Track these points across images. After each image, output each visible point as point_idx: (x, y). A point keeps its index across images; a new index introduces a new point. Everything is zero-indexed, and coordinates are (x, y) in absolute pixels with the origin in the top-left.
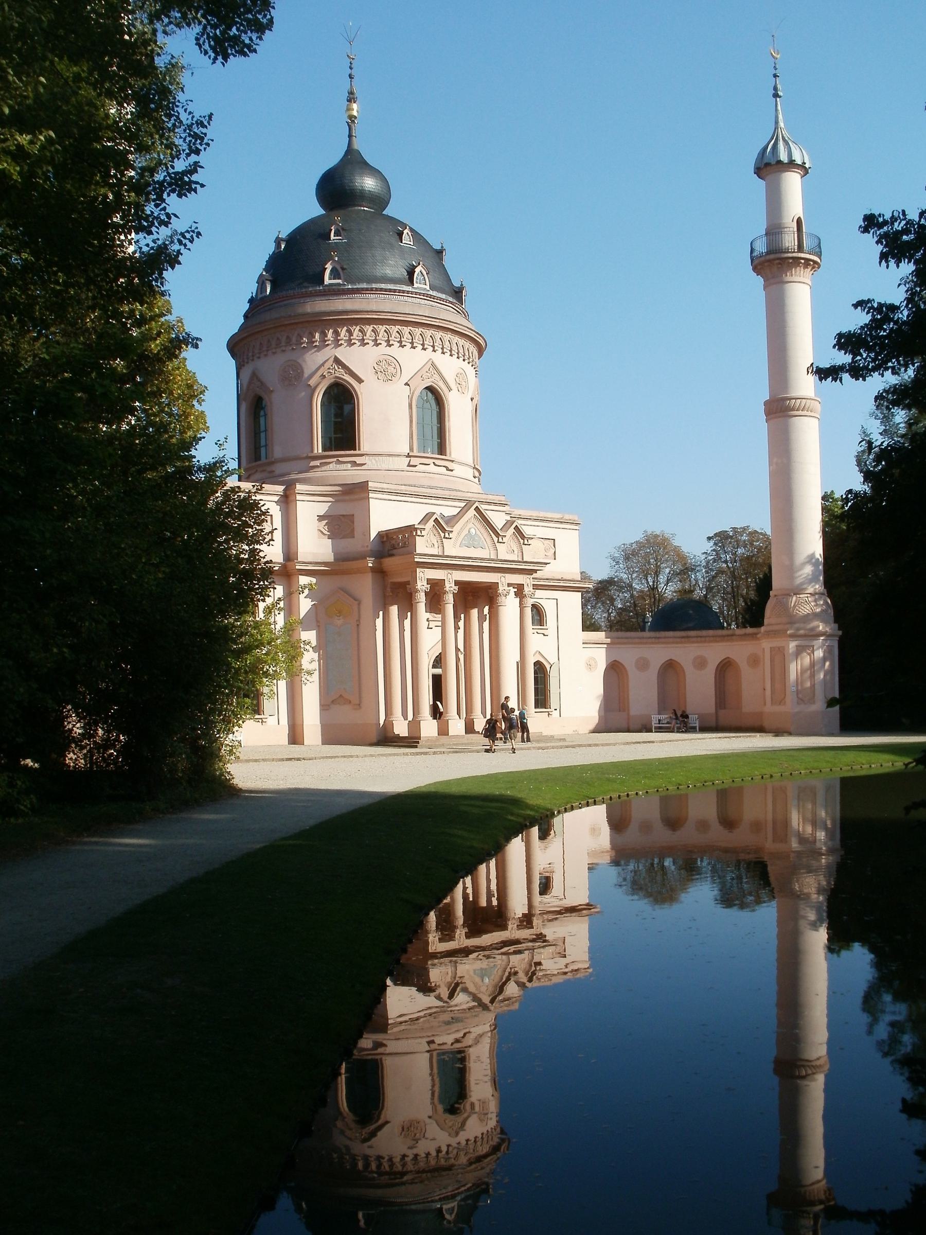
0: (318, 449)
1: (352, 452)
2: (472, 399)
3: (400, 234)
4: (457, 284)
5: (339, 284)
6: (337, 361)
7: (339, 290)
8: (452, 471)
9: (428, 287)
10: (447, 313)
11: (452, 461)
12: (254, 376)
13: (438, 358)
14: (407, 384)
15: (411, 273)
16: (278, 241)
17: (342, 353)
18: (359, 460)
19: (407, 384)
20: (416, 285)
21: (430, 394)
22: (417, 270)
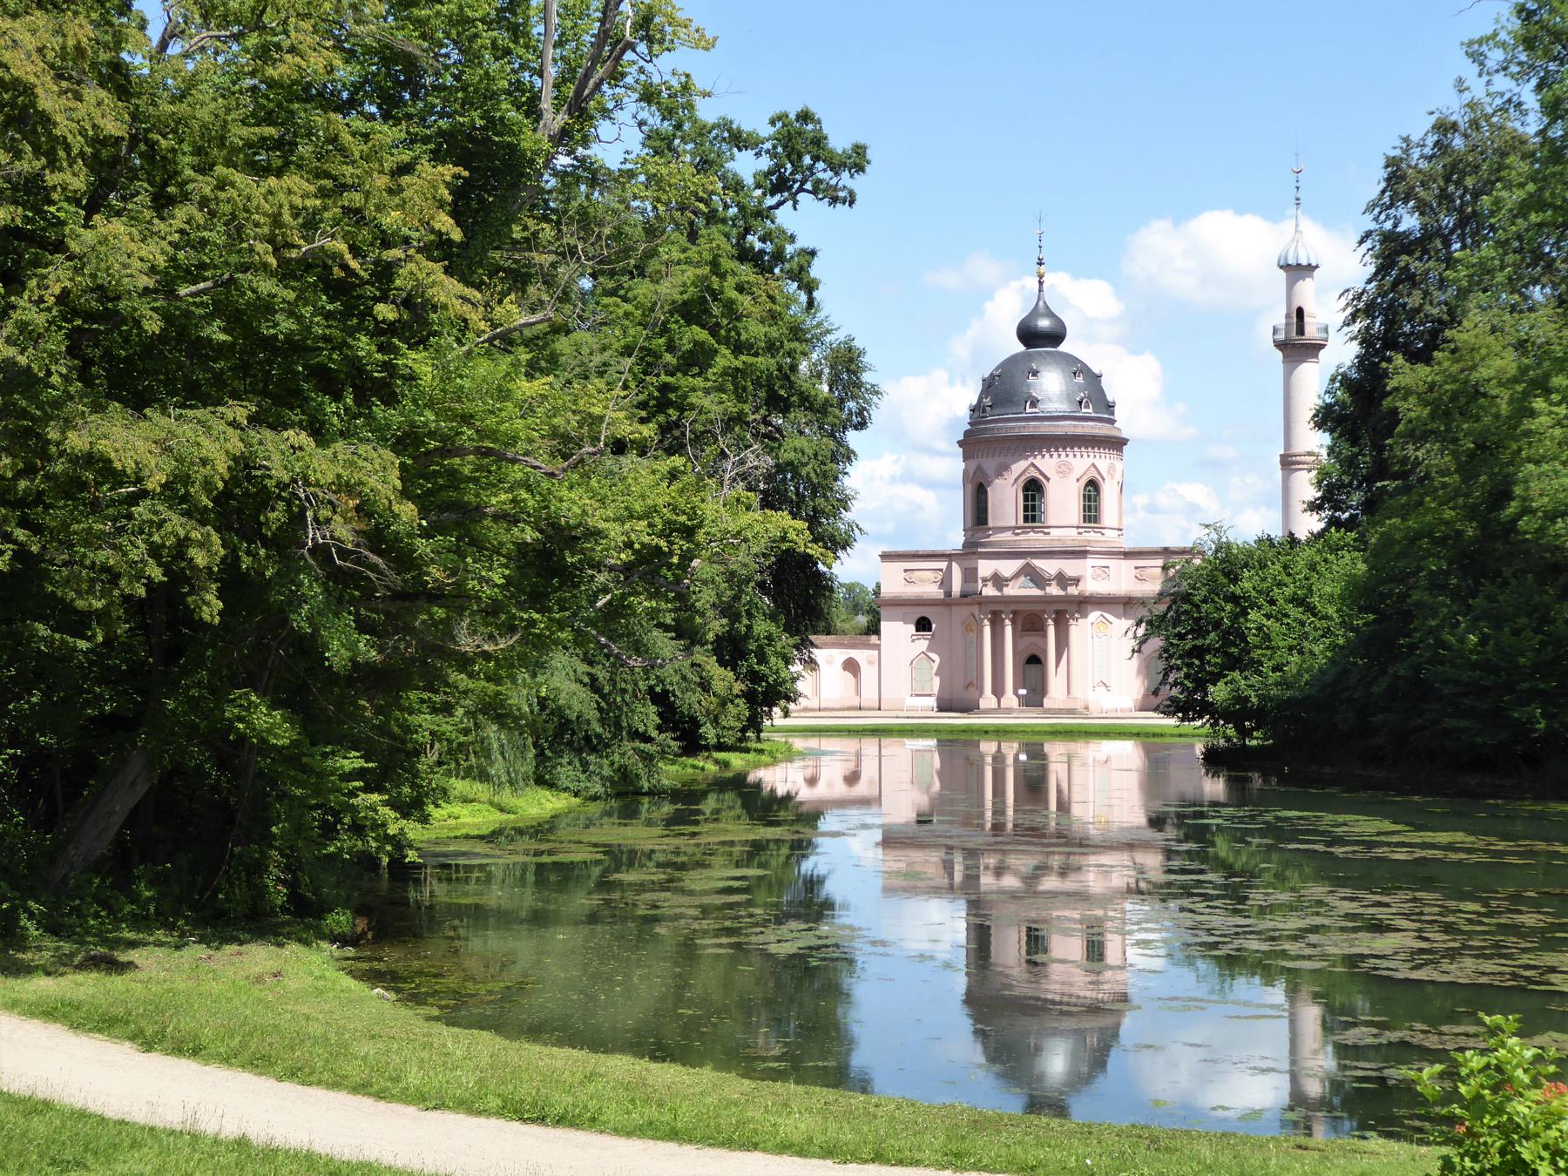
0: (1021, 522)
6: (1033, 465)
12: (979, 469)
15: (1080, 402)
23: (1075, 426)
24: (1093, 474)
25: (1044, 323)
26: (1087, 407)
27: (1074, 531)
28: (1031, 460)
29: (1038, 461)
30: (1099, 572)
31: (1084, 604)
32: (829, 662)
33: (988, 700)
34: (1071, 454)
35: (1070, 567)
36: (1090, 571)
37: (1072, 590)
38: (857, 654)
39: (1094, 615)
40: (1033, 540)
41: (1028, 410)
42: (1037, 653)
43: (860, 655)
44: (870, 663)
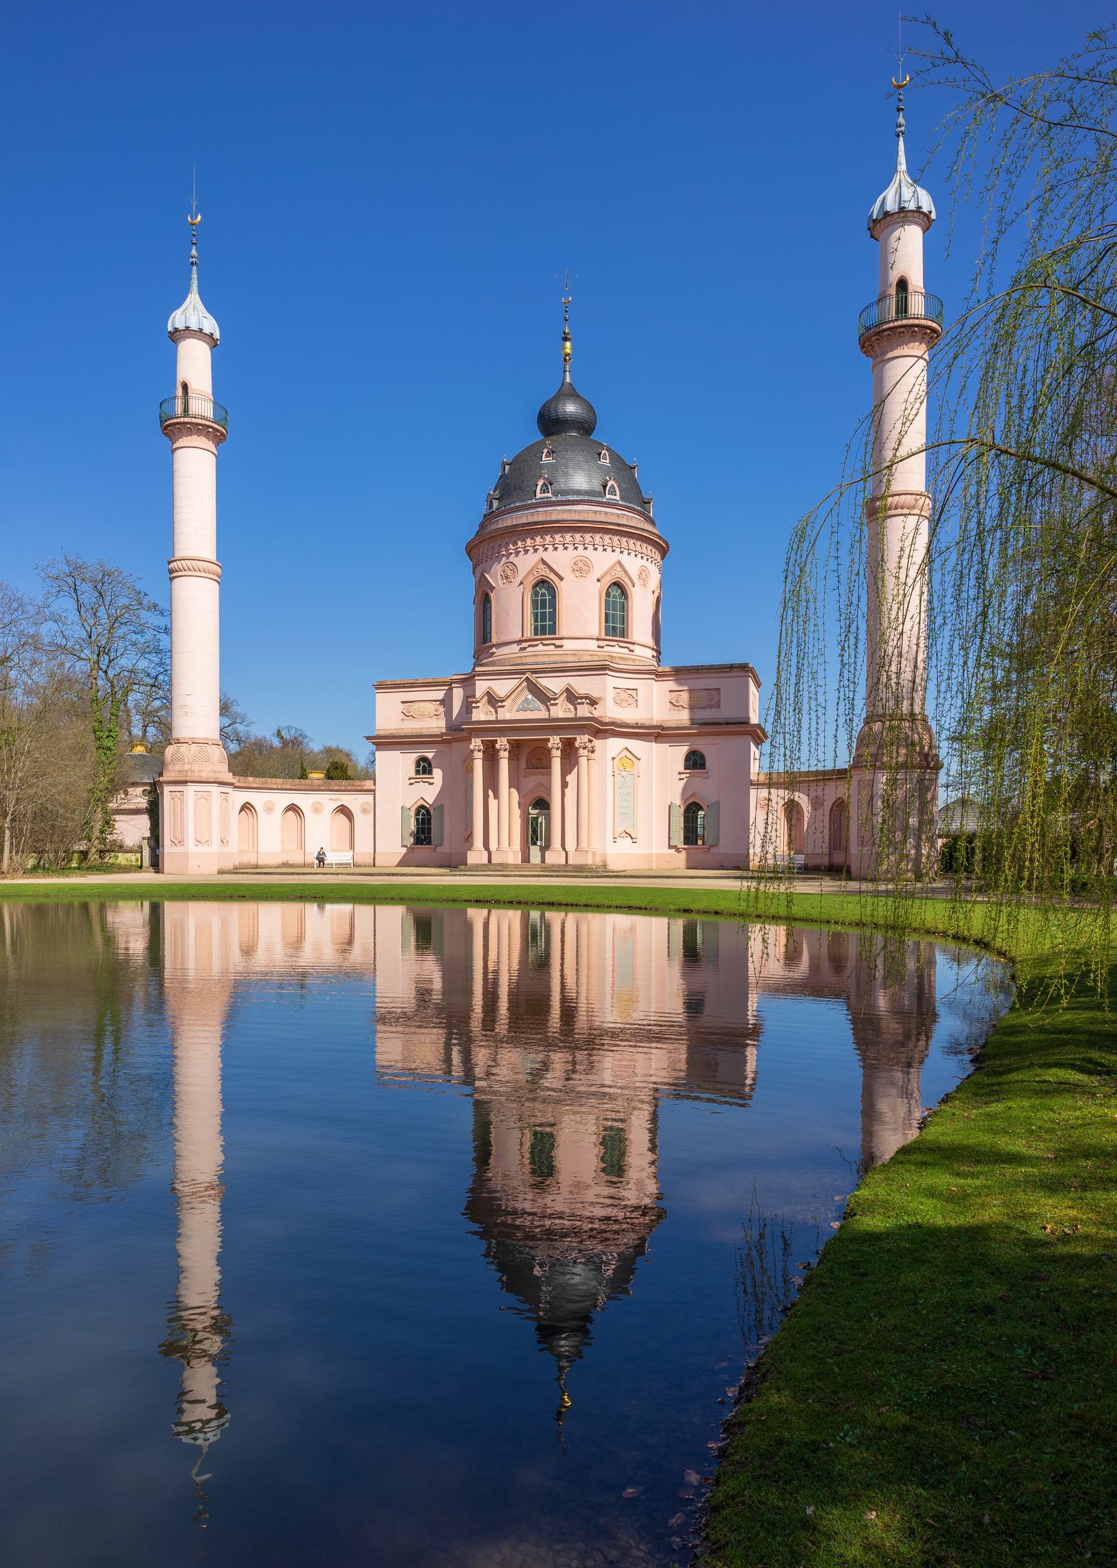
0: (529, 633)
1: (552, 636)
2: (653, 592)
3: (599, 454)
4: (646, 496)
5: (548, 498)
6: (543, 562)
7: (547, 502)
8: (633, 651)
9: (618, 498)
10: (635, 521)
11: (634, 644)
13: (625, 559)
14: (598, 580)
15: (605, 487)
16: (504, 464)
17: (549, 556)
18: (557, 642)
19: (598, 580)
20: (608, 496)
21: (615, 588)
22: (609, 484)
23: (595, 512)
24: (619, 574)
25: (571, 408)
26: (613, 493)
27: (595, 643)
28: (541, 553)
29: (549, 556)
30: (623, 695)
31: (602, 730)
32: (317, 810)
33: (476, 856)
34: (591, 548)
35: (582, 685)
36: (610, 695)
37: (584, 711)
38: (347, 799)
39: (614, 745)
40: (543, 652)
41: (539, 495)
42: (545, 797)
43: (353, 801)
44: (365, 811)
